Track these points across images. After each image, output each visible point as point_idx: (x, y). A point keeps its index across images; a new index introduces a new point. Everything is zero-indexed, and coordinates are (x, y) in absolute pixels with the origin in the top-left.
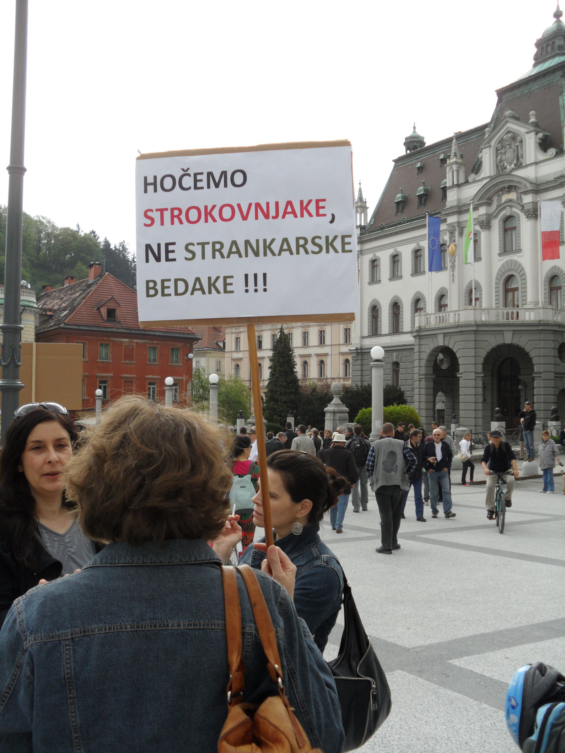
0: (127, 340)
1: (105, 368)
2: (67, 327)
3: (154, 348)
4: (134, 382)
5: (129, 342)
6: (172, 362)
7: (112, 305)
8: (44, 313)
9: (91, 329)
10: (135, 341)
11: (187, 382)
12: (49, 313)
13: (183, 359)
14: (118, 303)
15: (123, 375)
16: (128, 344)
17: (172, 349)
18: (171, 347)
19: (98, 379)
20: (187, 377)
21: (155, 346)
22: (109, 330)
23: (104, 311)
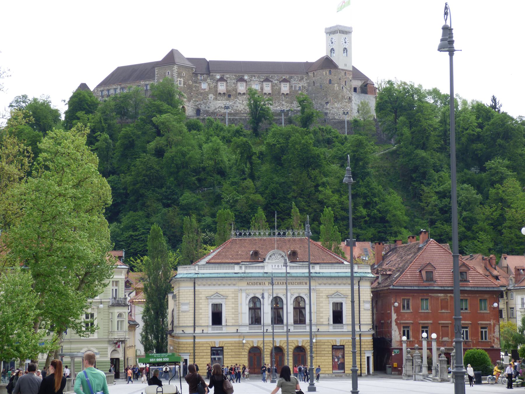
0: (442, 295)
1: (426, 316)
2: (395, 288)
3: (467, 300)
4: (449, 327)
5: (444, 296)
6: (481, 309)
7: (429, 269)
8: (384, 273)
9: (413, 288)
10: (449, 295)
11: (494, 325)
12: (388, 273)
13: (490, 307)
14: (434, 267)
15: (440, 322)
16: (443, 298)
17: (480, 300)
18: (479, 298)
19: (421, 325)
20: (494, 321)
21: (466, 298)
22: (427, 288)
23: (424, 273)
